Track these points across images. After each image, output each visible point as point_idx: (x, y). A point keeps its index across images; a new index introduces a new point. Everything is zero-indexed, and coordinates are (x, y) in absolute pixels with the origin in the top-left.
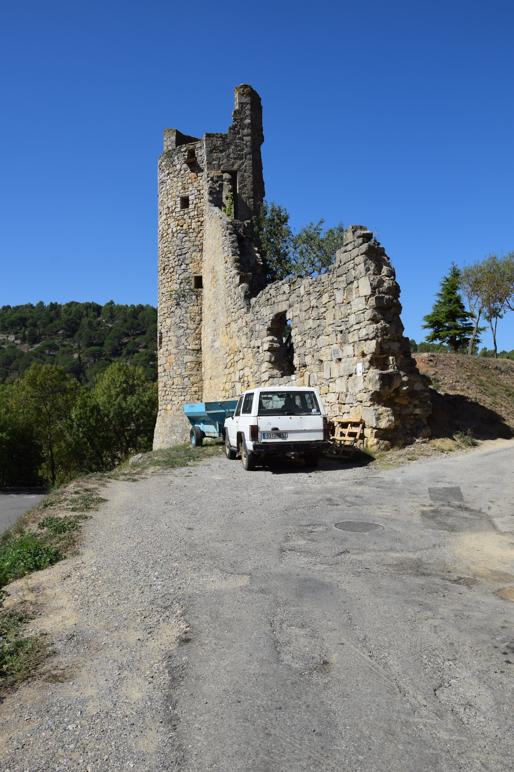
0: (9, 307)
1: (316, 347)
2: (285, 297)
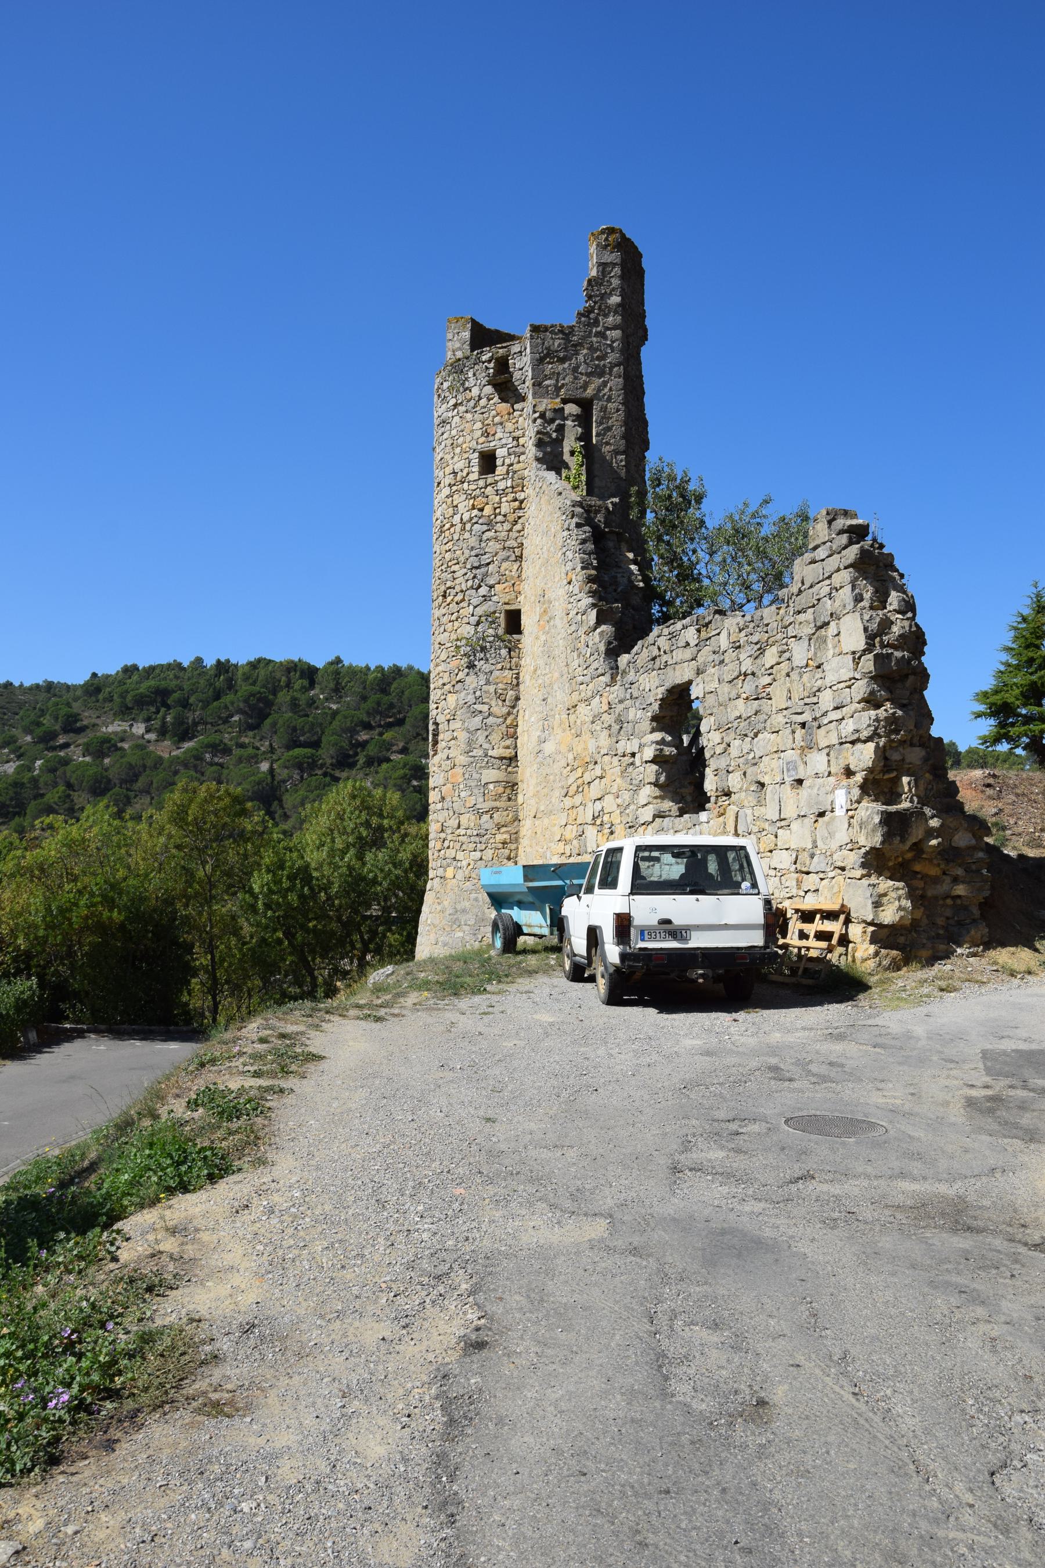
0: (135, 667)
1: (752, 755)
2: (688, 654)
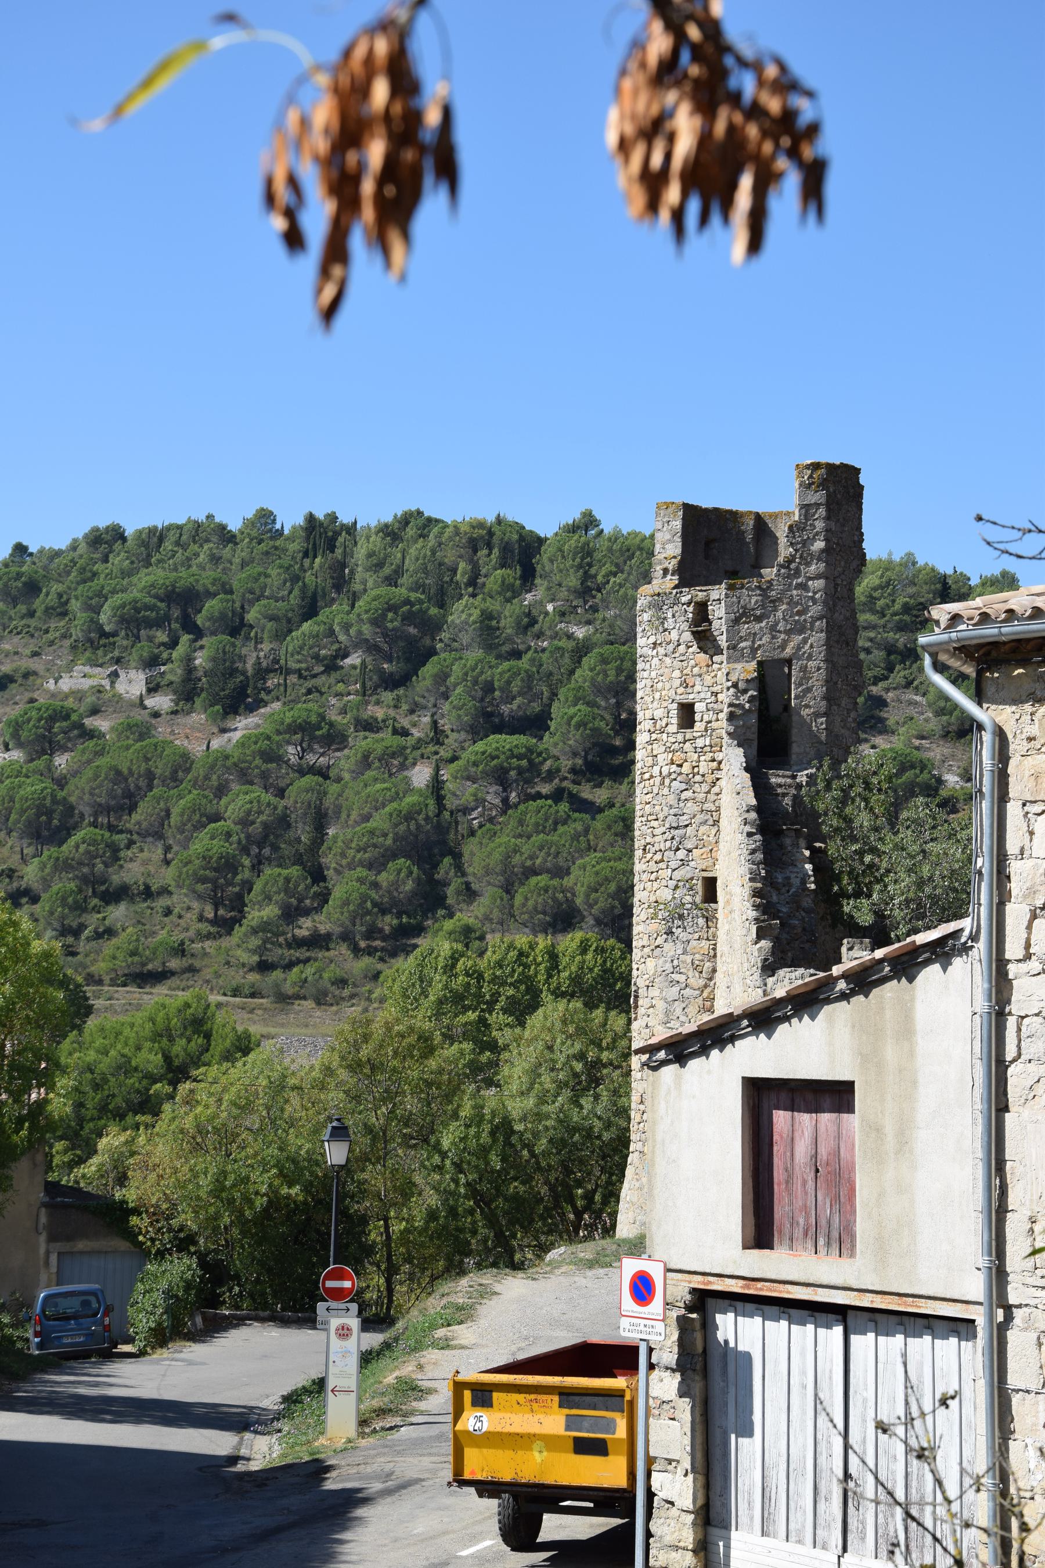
0: (116, 534)
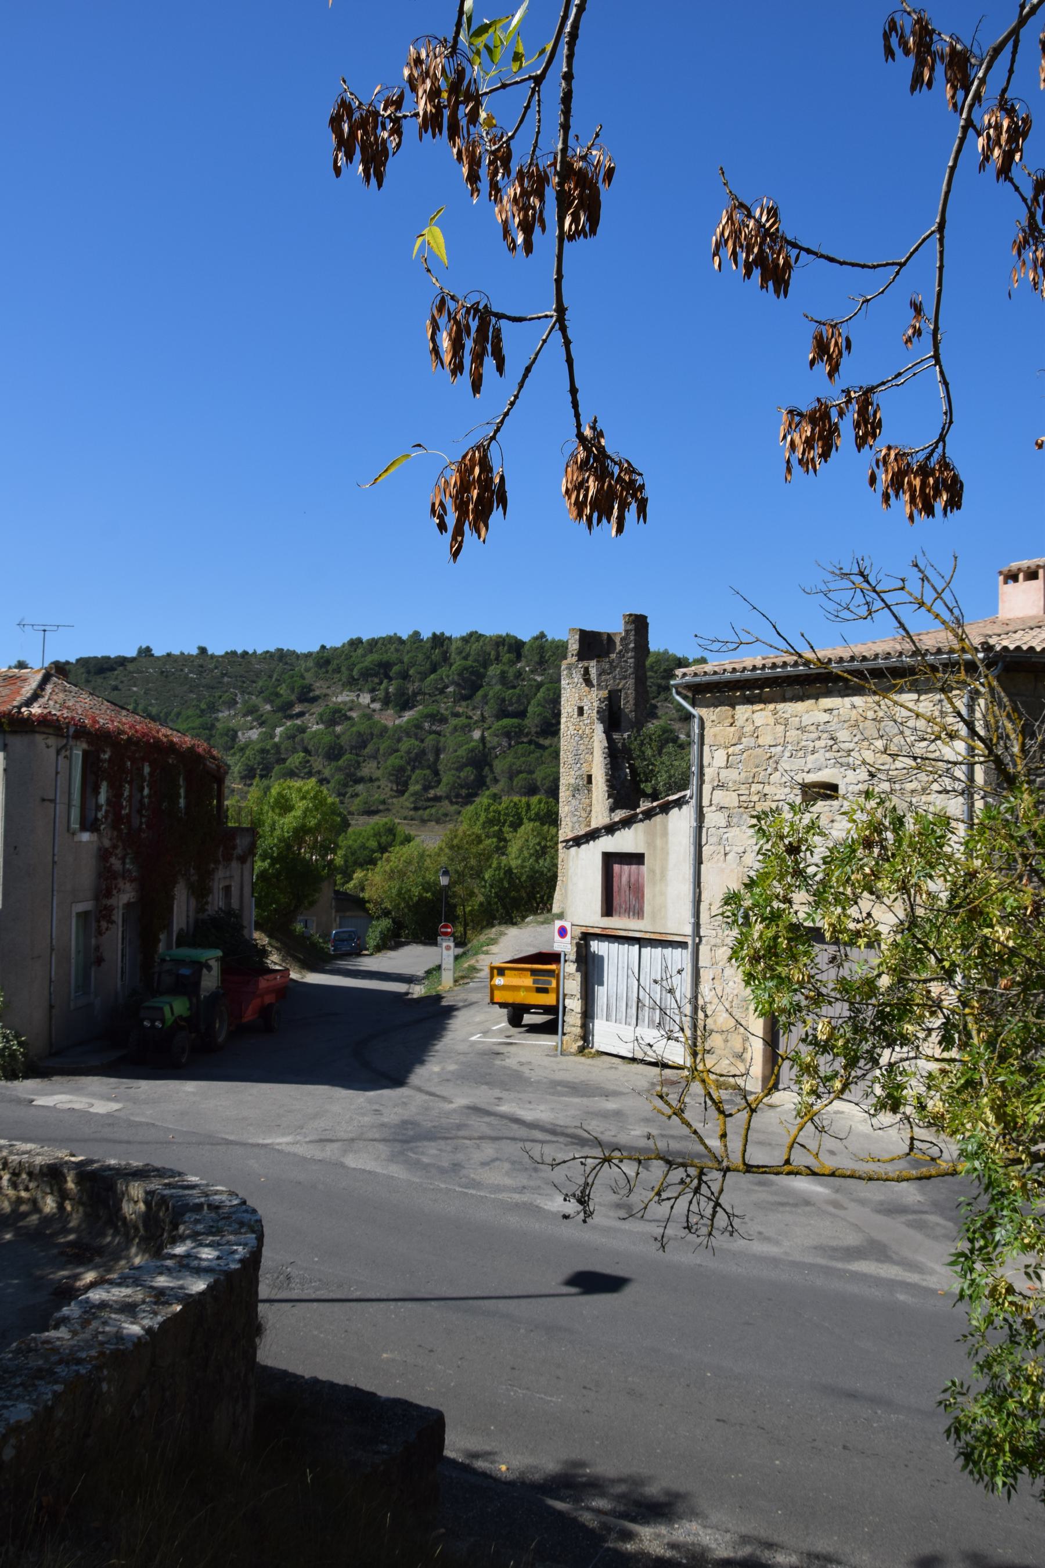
0: (359, 641)
